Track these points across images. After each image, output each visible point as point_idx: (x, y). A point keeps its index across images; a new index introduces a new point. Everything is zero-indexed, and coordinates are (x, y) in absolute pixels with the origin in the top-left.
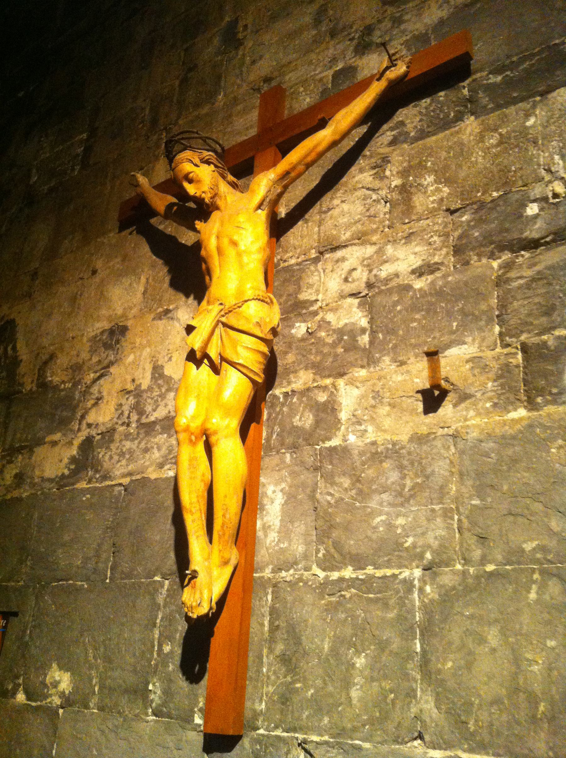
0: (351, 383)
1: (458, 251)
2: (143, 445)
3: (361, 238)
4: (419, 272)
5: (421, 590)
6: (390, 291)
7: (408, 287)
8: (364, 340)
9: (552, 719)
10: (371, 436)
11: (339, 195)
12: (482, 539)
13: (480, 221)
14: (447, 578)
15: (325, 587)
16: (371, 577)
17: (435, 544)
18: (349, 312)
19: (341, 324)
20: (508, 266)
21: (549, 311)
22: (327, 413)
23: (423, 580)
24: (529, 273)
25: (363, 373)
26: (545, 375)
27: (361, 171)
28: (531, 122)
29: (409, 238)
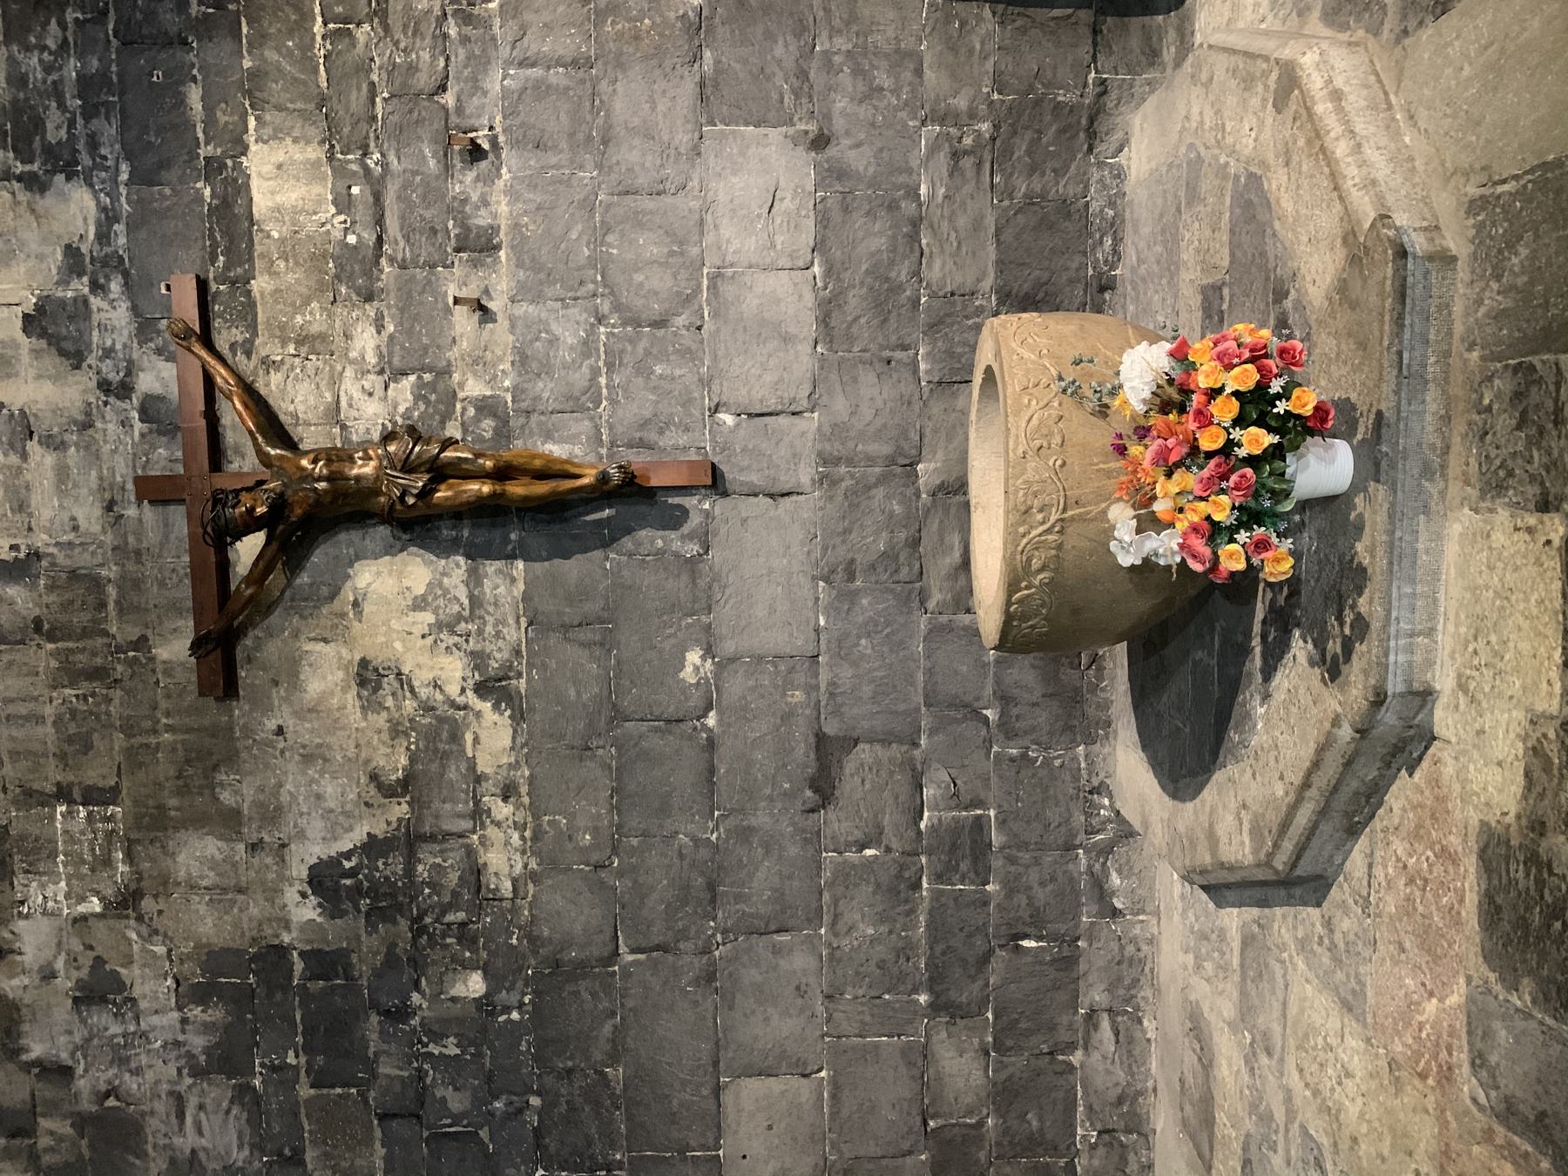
0: (461, 385)
1: (369, 298)
2: (491, 609)
3: (335, 380)
4: (380, 328)
5: (613, 326)
6: (391, 354)
7: (391, 337)
8: (427, 377)
9: (681, 244)
10: (507, 366)
11: (283, 405)
12: (581, 283)
13: (351, 277)
14: (605, 306)
15: (613, 402)
16: (606, 364)
17: (585, 315)
18: (402, 391)
19: (410, 397)
20: (392, 260)
21: (434, 231)
22: (486, 407)
23: (606, 326)
24: (402, 243)
25: (456, 377)
26: (479, 237)
27: (267, 385)
28: (275, 235)
29: (347, 336)
